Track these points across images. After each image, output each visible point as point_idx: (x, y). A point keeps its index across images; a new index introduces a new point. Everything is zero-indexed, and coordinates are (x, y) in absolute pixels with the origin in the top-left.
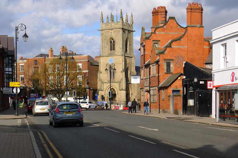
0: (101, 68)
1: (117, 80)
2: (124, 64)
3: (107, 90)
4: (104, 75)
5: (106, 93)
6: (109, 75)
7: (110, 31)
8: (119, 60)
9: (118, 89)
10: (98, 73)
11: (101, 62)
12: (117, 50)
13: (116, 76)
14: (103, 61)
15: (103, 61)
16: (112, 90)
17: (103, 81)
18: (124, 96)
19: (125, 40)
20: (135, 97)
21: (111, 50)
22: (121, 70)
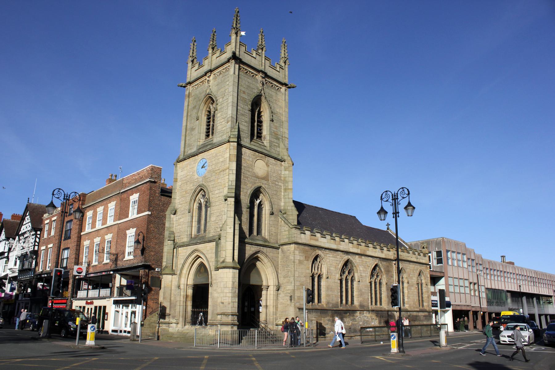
0: (178, 198)
1: (212, 231)
2: (235, 168)
3: (185, 271)
4: (182, 220)
5: (183, 281)
6: (195, 219)
7: (208, 79)
8: (221, 160)
9: (213, 268)
10: (167, 213)
11: (179, 180)
12: (219, 127)
13: (210, 217)
14: (182, 173)
15: (182, 173)
16: (202, 269)
17: (177, 240)
18: (227, 290)
19: (249, 98)
20: (288, 298)
21: (208, 136)
22: (225, 191)
